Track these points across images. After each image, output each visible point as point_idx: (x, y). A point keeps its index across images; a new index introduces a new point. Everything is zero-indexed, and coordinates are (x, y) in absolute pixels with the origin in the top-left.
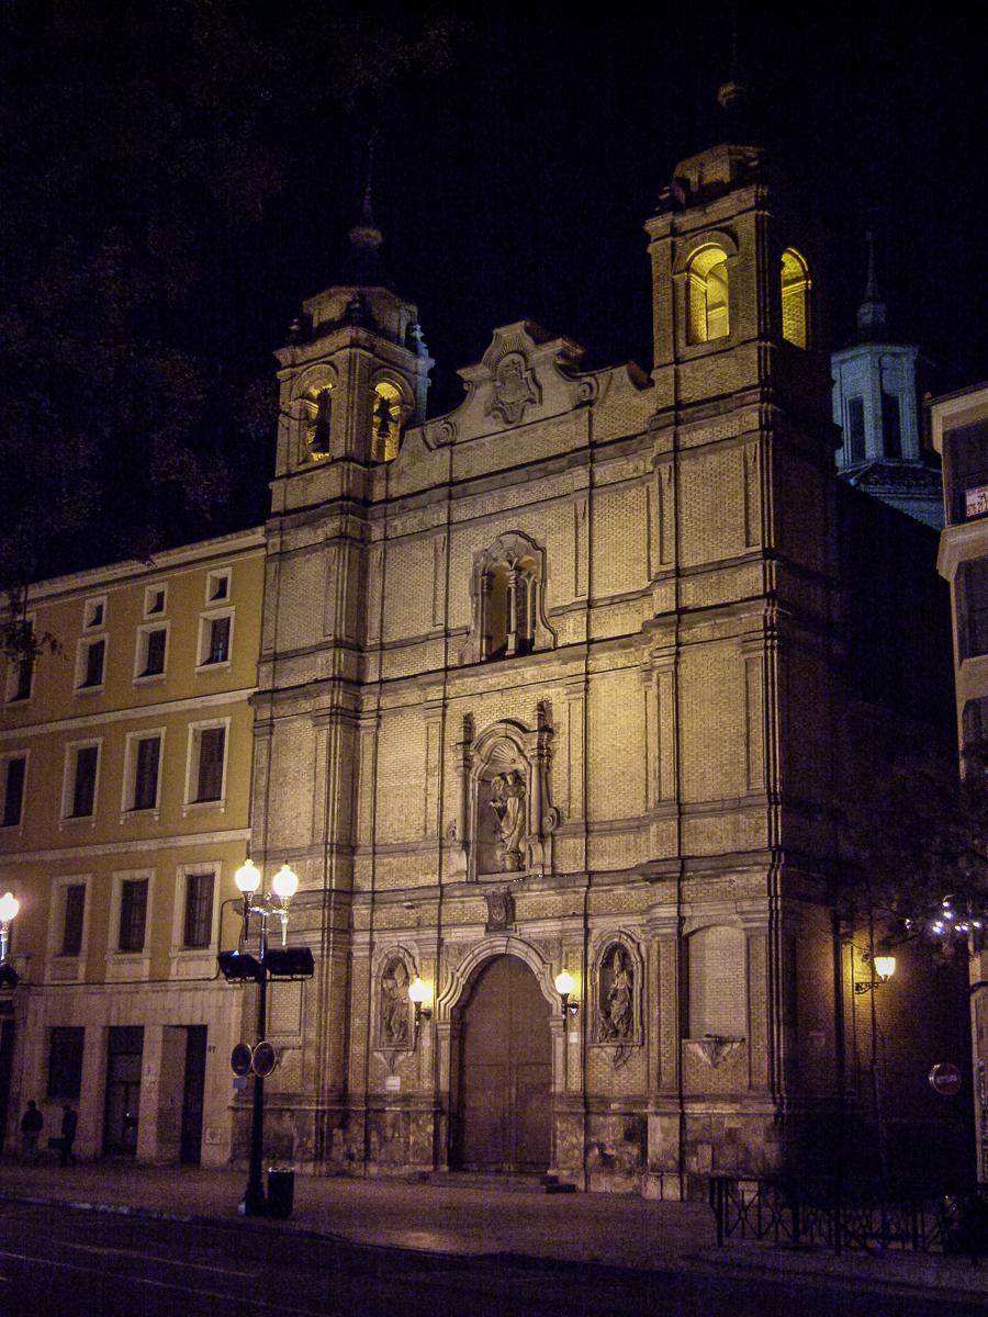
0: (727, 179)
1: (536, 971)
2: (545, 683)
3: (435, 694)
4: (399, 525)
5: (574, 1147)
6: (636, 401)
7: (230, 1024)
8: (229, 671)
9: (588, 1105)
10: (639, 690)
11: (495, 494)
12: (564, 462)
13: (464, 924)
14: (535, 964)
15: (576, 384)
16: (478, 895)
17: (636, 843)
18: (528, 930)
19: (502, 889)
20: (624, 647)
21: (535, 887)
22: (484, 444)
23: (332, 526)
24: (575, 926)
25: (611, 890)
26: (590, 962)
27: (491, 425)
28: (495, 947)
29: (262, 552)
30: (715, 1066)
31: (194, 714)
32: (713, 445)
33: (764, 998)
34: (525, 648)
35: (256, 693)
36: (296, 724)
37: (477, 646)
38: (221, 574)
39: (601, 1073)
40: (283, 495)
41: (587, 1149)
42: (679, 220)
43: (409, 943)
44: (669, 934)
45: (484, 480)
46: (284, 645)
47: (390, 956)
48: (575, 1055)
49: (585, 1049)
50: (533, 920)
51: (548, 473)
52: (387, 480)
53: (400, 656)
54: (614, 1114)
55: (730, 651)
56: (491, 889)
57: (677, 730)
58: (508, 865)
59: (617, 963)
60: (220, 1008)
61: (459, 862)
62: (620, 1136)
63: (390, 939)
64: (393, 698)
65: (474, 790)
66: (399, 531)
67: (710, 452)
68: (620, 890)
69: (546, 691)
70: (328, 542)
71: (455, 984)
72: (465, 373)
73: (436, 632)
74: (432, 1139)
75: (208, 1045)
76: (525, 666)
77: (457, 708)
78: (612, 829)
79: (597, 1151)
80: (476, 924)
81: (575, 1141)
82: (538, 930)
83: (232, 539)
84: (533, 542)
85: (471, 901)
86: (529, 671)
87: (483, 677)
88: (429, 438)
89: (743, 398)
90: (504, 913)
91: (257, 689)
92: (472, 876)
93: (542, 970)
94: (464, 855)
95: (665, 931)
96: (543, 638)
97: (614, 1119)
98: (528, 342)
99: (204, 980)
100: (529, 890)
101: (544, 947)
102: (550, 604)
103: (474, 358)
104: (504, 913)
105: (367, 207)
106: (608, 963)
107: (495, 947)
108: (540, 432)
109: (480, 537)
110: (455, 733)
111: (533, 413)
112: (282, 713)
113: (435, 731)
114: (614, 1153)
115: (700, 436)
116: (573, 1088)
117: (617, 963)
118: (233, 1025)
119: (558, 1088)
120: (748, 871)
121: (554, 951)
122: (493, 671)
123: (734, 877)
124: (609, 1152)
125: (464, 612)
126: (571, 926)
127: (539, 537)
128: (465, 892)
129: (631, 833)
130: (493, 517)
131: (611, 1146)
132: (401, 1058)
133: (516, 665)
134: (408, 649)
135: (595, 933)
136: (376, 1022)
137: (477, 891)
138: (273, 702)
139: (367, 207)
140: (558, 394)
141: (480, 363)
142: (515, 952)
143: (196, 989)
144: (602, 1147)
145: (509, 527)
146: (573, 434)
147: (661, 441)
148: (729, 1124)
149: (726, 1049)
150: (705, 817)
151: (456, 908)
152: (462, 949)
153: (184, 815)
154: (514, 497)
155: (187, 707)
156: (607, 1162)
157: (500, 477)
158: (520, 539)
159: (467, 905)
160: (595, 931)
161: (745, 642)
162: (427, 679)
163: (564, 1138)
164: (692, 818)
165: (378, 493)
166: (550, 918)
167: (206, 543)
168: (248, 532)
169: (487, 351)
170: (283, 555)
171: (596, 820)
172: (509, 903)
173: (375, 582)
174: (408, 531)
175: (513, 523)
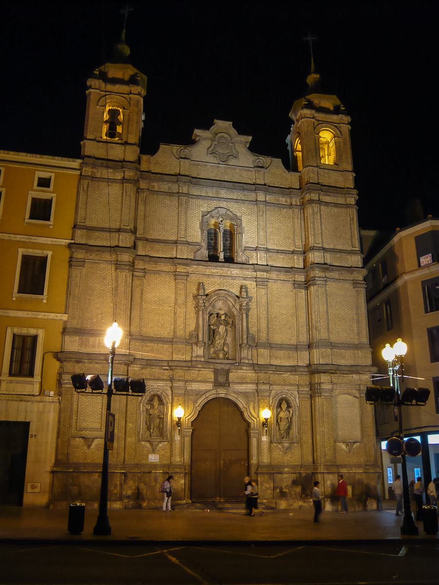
0: (332, 109)
1: (241, 406)
2: (245, 279)
3: (181, 269)
4: (156, 186)
5: (268, 488)
6: (284, 174)
7: (48, 423)
8: (51, 227)
9: (273, 470)
10: (292, 291)
11: (215, 189)
12: (253, 187)
13: (199, 381)
14: (241, 403)
15: (257, 158)
16: (209, 368)
17: (293, 355)
18: (238, 388)
19: (227, 367)
20: (286, 272)
21: (245, 368)
22: (207, 166)
23: (129, 174)
24: (265, 388)
25: (282, 374)
27: (210, 159)
28: (218, 394)
29: (78, 172)
30: (349, 452)
31: (24, 245)
32: (336, 205)
34: (230, 260)
35: (71, 243)
36: (102, 266)
37: (204, 253)
38: (44, 175)
39: (277, 454)
40: (89, 148)
41: (274, 489)
42: (316, 115)
43: (164, 387)
44: (328, 396)
45: (211, 181)
46: (94, 224)
47: (152, 393)
48: (265, 447)
49: (271, 442)
50: (239, 383)
51: (244, 189)
52: (149, 163)
53: (157, 246)
54: (286, 473)
55: (348, 286)
56: (219, 367)
57: (327, 312)
58: (221, 356)
59: (284, 406)
60: (41, 412)
61: (199, 351)
62: (290, 483)
63: (153, 384)
64: (153, 266)
65: (206, 318)
66: (156, 188)
67: (334, 206)
68: (286, 375)
69: (245, 282)
70: (124, 180)
71: (195, 409)
72: (197, 132)
73: (181, 241)
74: (183, 487)
75: (30, 433)
76: (234, 268)
77: (194, 278)
78: (281, 347)
79: (278, 490)
80: (206, 382)
81: (268, 486)
82: (242, 388)
83: (58, 160)
84: (236, 215)
85: (205, 371)
86: (235, 271)
87: (210, 268)
88: (175, 151)
89: (349, 191)
90: (222, 380)
91: (73, 241)
93: (246, 406)
94: (203, 348)
95: (326, 394)
96: (240, 257)
97: (286, 475)
98: (233, 131)
99: (29, 395)
100: (241, 369)
101: (245, 395)
102: (244, 244)
103: (207, 126)
104: (222, 380)
105: (123, 36)
106: (279, 406)
107: (218, 394)
108: (237, 171)
109: (206, 205)
110: (193, 290)
111: (233, 162)
112: (91, 257)
114: (287, 491)
115: (327, 199)
116: (265, 461)
117: (284, 406)
118: (51, 424)
119: (254, 461)
120: (364, 373)
121: (257, 397)
122: (216, 266)
123: (354, 376)
124: (285, 490)
125: (196, 235)
126: (262, 388)
127: (239, 214)
128: (205, 366)
129: (290, 350)
130: (213, 198)
132: (160, 445)
133: (231, 266)
134: (164, 244)
135: (273, 392)
136: (143, 426)
137: (212, 367)
138: (87, 251)
139: (123, 36)
140: (246, 159)
141: (209, 130)
142: (231, 398)
143: (21, 401)
144: (281, 489)
145: (221, 205)
146: (248, 177)
147: (313, 195)
148: (357, 477)
149: (355, 446)
150: (340, 349)
151: (193, 373)
152: (199, 394)
153: (14, 299)
154: (223, 193)
155: (18, 239)
156: (283, 495)
157: (220, 183)
158: (228, 212)
159: (200, 372)
160: (273, 391)
161: (355, 283)
162: (179, 261)
164: (335, 349)
165: (144, 166)
166: (249, 383)
167: (38, 156)
168: (71, 160)
169: (212, 127)
170: (93, 178)
171: (272, 342)
172: (227, 372)
173: (141, 207)
174: (162, 190)
175: (224, 204)
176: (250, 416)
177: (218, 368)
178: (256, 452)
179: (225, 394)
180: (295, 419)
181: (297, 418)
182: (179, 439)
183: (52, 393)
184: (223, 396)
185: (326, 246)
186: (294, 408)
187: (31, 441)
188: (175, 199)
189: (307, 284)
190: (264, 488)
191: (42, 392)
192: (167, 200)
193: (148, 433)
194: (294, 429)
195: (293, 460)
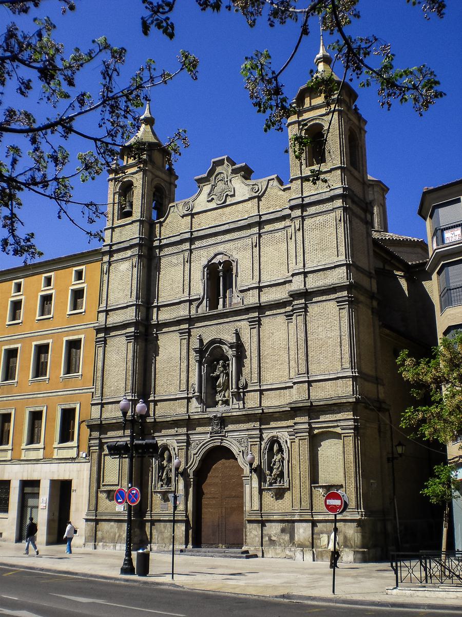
5: (256, 536)
26: (262, 449)
33: (353, 465)
60: (78, 471)
63: (163, 439)
79: (267, 538)
81: (256, 533)
92: (203, 409)
113: (185, 342)
117: (276, 447)
124: (273, 538)
125: (199, 288)
131: (274, 535)
163: (251, 532)
183: (84, 456)
184: (219, 444)
187: (73, 495)
189: (289, 316)
190: (252, 536)
191: (78, 455)
193: (160, 483)
195: (284, 506)
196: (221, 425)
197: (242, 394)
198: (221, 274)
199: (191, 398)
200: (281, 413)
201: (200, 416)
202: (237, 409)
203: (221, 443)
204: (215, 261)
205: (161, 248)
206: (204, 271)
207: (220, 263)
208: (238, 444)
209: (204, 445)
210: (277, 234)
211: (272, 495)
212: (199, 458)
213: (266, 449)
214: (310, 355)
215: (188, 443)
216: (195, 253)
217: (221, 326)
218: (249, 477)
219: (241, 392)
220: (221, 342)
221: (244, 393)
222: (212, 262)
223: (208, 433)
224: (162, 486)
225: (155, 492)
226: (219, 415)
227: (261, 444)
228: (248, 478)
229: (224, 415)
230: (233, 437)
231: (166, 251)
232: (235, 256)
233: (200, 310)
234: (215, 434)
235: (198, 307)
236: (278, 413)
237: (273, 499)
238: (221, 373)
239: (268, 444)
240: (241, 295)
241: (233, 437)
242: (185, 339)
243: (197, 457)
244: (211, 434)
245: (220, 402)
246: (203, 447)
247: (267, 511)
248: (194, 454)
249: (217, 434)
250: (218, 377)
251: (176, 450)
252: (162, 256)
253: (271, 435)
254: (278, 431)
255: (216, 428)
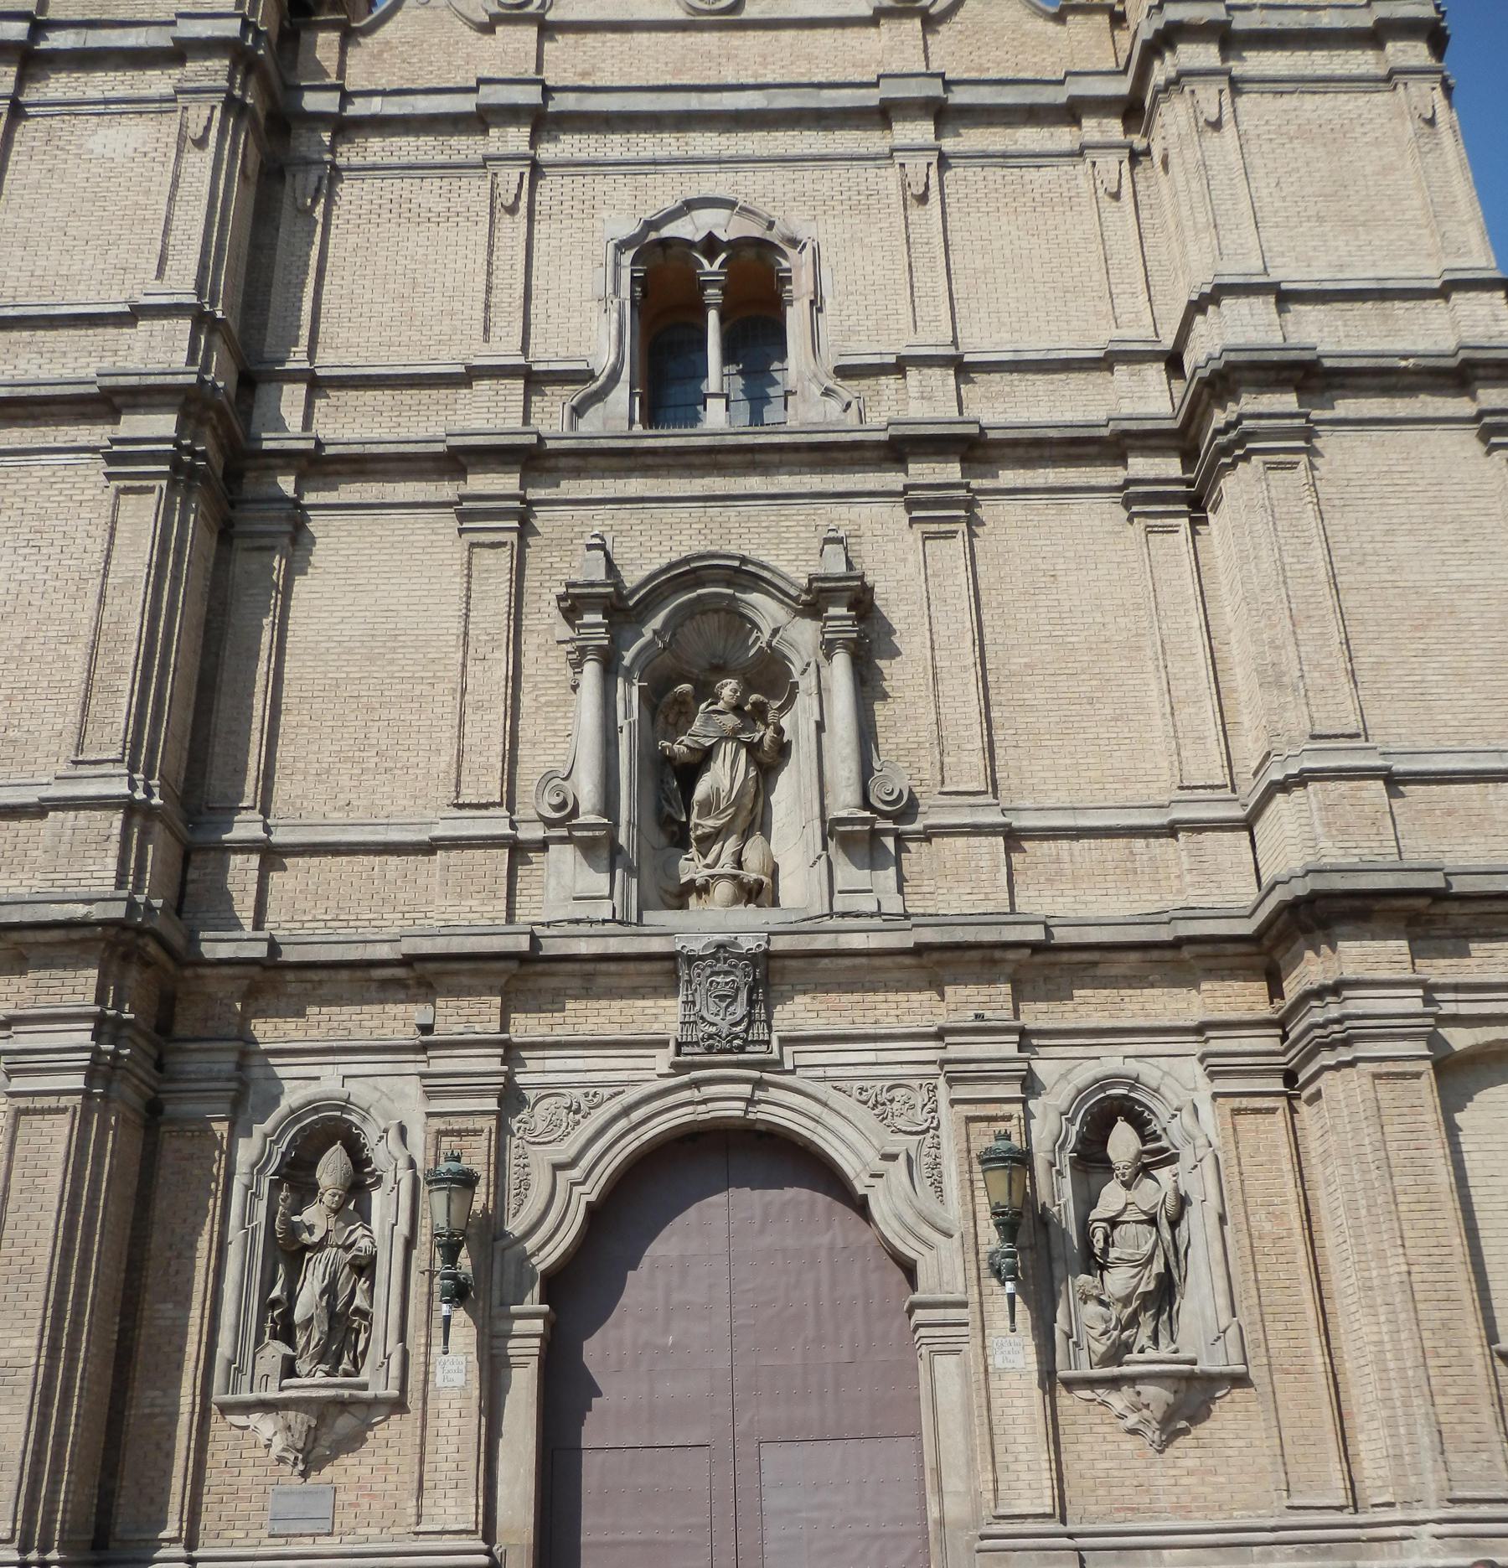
25: (1095, 964)
85: (619, 974)
113: (498, 564)
117: (1123, 1143)
176: (910, 1218)
177: (697, 946)
178: (959, 1437)
179: (750, 1101)
180: (1199, 1225)
181: (1213, 1220)
182: (459, 1379)
184: (735, 1109)
185: (1289, 274)
186: (1187, 1157)
188: (473, 192)
192: (429, 193)
194: (1206, 1289)
196: (751, 1003)
197: (890, 842)
198: (713, 294)
199: (543, 845)
200: (1155, 955)
201: (614, 946)
202: (872, 915)
203: (746, 1112)
204: (688, 229)
205: (346, 127)
206: (617, 265)
207: (711, 245)
208: (865, 1117)
209: (626, 1111)
210: (1032, 174)
211: (1132, 1420)
212: (591, 1192)
213: (1062, 1147)
214: (1363, 659)
215: (511, 1099)
216: (548, 188)
217: (732, 512)
218: (963, 1305)
219: (886, 832)
220: (745, 575)
221: (900, 839)
222: (668, 231)
223: (664, 1044)
224: (289, 1370)
225: (226, 1409)
226: (748, 944)
227: (1028, 1115)
228: (953, 1314)
229: (780, 944)
230: (831, 1072)
231: (376, 148)
232: (795, 220)
233: (588, 425)
234: (709, 1050)
235: (578, 411)
236: (1134, 956)
237: (1130, 1444)
238: (724, 739)
239: (1071, 1121)
240: (848, 389)
241: (831, 1072)
242: (502, 544)
243: (574, 1184)
244: (678, 1054)
245: (723, 890)
246: (623, 1124)
247: (1101, 1517)
248: (557, 1167)
249: (722, 1051)
250: (704, 758)
251: (416, 1136)
252: (350, 169)
253: (1086, 1073)
254: (1131, 1050)
255: (722, 1019)
